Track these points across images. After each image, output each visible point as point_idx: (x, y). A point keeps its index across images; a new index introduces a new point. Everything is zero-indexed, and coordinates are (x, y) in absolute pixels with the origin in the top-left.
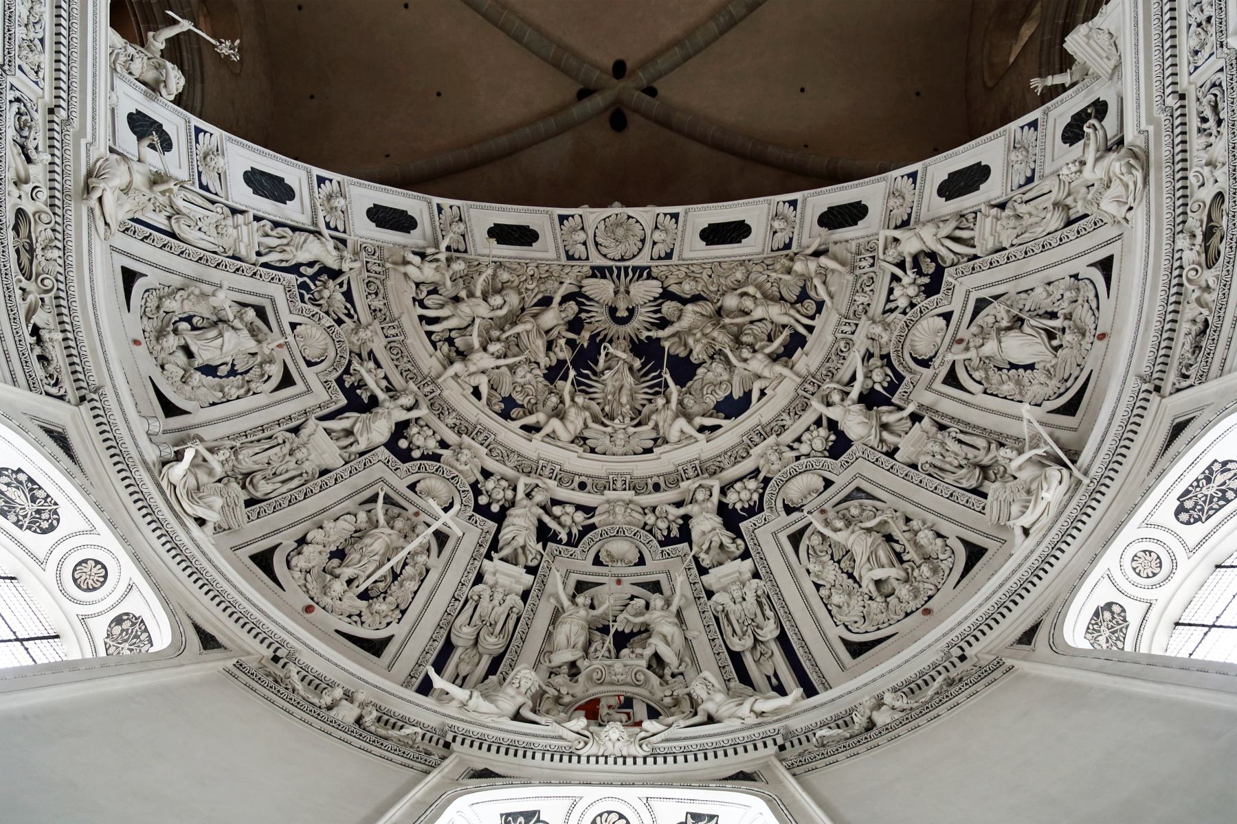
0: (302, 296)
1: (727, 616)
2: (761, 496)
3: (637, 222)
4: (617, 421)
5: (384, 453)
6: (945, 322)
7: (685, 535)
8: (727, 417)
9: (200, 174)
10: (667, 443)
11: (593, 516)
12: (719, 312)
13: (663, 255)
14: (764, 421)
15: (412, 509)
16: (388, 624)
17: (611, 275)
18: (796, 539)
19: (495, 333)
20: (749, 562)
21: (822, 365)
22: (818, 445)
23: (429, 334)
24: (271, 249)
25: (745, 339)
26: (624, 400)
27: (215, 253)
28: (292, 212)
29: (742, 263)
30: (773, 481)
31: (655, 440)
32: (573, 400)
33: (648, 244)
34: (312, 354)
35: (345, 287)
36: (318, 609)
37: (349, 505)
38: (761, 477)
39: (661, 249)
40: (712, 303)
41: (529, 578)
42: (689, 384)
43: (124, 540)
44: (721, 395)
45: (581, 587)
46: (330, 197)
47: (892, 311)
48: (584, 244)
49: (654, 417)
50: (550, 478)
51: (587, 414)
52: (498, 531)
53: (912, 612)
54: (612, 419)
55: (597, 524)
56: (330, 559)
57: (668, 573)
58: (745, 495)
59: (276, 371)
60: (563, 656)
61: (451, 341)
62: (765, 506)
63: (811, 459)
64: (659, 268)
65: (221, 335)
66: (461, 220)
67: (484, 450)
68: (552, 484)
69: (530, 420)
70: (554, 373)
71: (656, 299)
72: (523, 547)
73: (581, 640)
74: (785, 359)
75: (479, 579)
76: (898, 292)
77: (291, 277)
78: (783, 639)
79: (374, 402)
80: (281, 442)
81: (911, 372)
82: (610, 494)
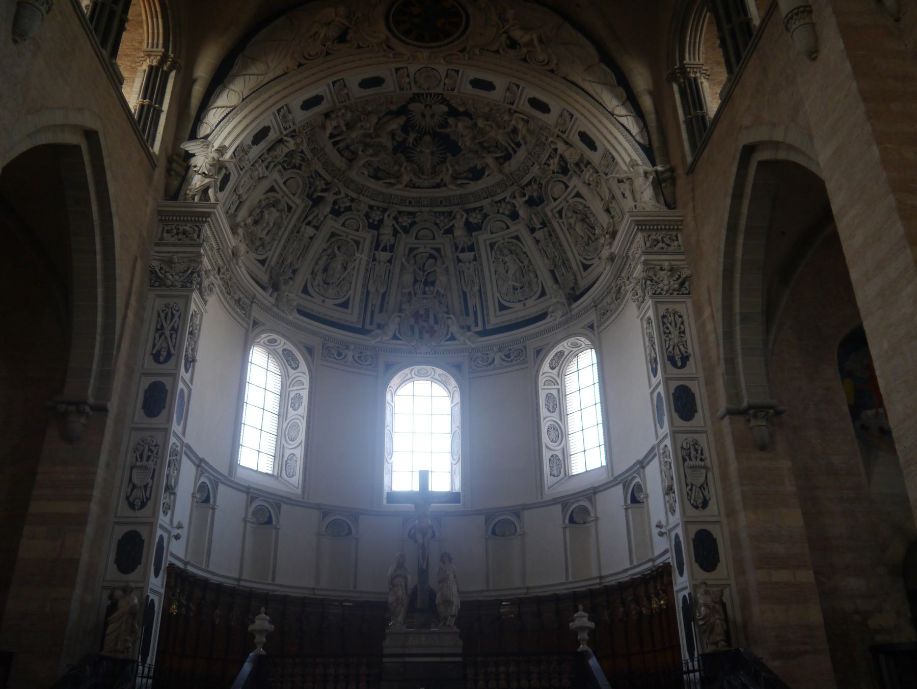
0: (283, 167)
1: (463, 272)
3: (437, 71)
4: (425, 177)
5: (330, 216)
6: (564, 189)
7: (450, 231)
9: (240, 167)
10: (445, 186)
11: (414, 218)
12: (476, 124)
13: (450, 89)
16: (347, 291)
17: (423, 96)
18: (492, 245)
19: (368, 140)
20: (474, 253)
22: (507, 212)
24: (270, 163)
25: (485, 144)
28: (272, 136)
30: (487, 219)
31: (442, 180)
32: (405, 168)
33: (442, 83)
36: (327, 300)
38: (483, 212)
40: (471, 119)
41: (392, 254)
42: (459, 156)
43: (278, 333)
45: (412, 250)
46: (284, 116)
48: (409, 83)
50: (396, 204)
52: (379, 235)
53: (521, 301)
54: (423, 174)
56: (323, 273)
58: (476, 221)
60: (406, 291)
63: (504, 216)
66: (345, 86)
69: (388, 181)
70: (395, 150)
71: (444, 112)
72: (389, 240)
73: (412, 280)
74: (501, 161)
75: (374, 260)
78: (480, 291)
80: (295, 238)
82: (423, 209)
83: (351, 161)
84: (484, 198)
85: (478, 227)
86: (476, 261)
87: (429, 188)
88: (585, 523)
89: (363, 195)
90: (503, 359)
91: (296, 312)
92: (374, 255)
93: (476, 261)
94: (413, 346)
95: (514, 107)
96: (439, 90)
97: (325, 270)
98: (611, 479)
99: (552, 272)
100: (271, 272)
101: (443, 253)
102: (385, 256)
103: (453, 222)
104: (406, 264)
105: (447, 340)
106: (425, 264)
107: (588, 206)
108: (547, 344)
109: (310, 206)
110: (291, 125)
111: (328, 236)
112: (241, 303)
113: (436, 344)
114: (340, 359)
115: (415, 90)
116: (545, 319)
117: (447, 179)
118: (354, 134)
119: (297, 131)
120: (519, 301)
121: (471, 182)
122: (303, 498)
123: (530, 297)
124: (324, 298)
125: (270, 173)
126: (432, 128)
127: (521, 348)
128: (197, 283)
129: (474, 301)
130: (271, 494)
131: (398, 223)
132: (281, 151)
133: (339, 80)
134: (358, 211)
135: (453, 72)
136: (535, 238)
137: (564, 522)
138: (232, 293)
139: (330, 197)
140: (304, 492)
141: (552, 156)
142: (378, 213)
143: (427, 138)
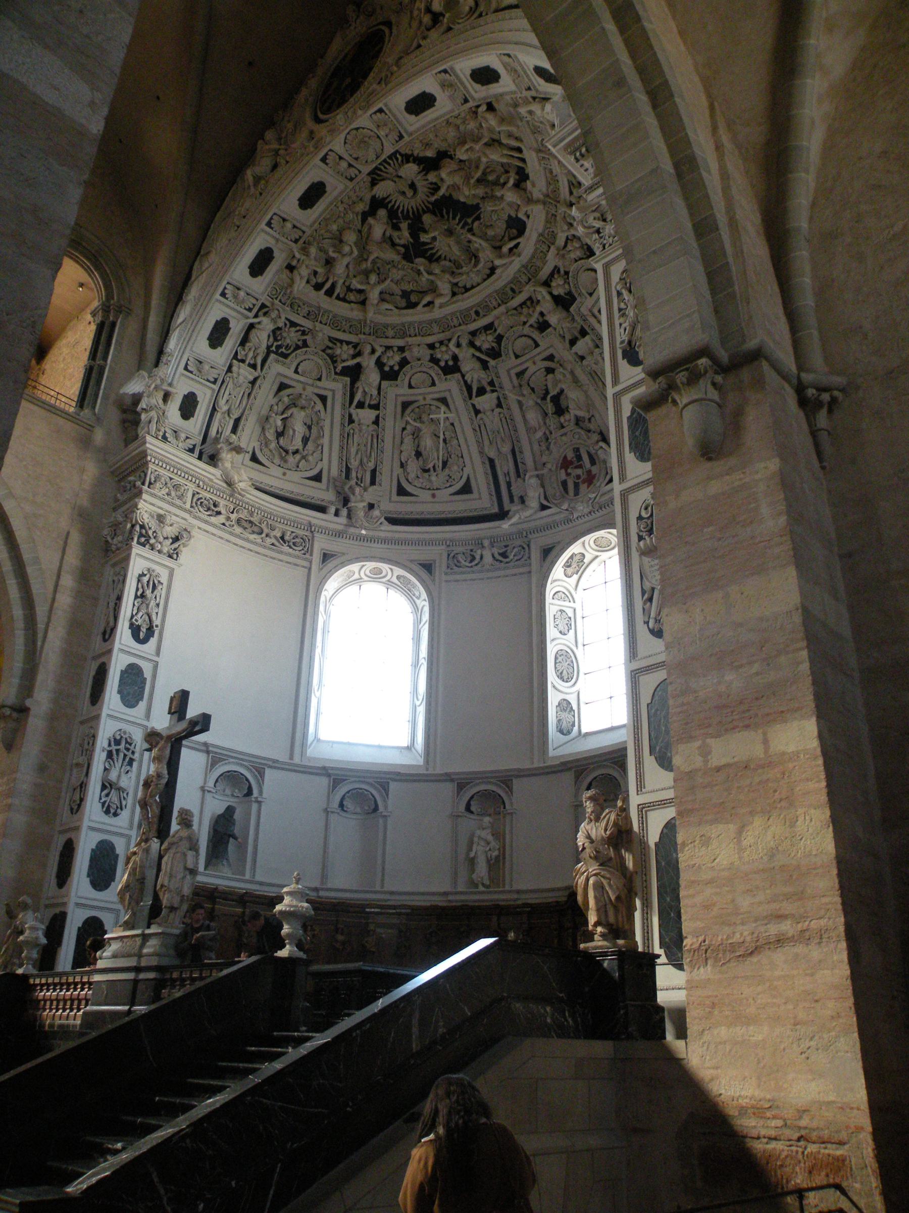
4: (464, 269)
5: (385, 384)
9: (208, 380)
11: (496, 330)
13: (397, 139)
14: (540, 231)
15: (420, 398)
17: (381, 170)
23: (338, 298)
25: (491, 178)
26: (458, 253)
27: (249, 395)
28: (237, 327)
34: (315, 374)
35: (287, 323)
37: (400, 424)
38: (562, 272)
46: (235, 297)
48: (350, 165)
50: (460, 325)
51: (447, 276)
52: (463, 376)
54: (459, 267)
55: (502, 333)
56: (418, 459)
59: (319, 406)
60: (539, 434)
61: (349, 289)
64: (402, 146)
65: (294, 431)
66: (284, 220)
67: (419, 338)
68: (462, 327)
69: (424, 302)
75: (477, 412)
77: (272, 356)
79: (359, 366)
82: (496, 312)
83: (363, 303)
87: (485, 280)
89: (410, 336)
91: (386, 523)
92: (474, 406)
94: (567, 510)
95: (471, 104)
96: (389, 150)
97: (418, 454)
100: (336, 486)
102: (486, 402)
103: (538, 309)
104: (520, 398)
106: (546, 385)
109: (349, 383)
110: (254, 301)
111: (399, 409)
112: (287, 538)
113: (594, 495)
114: (476, 565)
115: (366, 169)
118: (340, 269)
119: (268, 304)
122: (427, 770)
124: (431, 492)
125: (262, 369)
126: (428, 202)
128: (141, 535)
130: (368, 771)
131: (479, 349)
132: (261, 338)
133: (271, 218)
134: (419, 360)
135: (378, 114)
138: (266, 531)
139: (368, 362)
140: (427, 761)
143: (427, 219)
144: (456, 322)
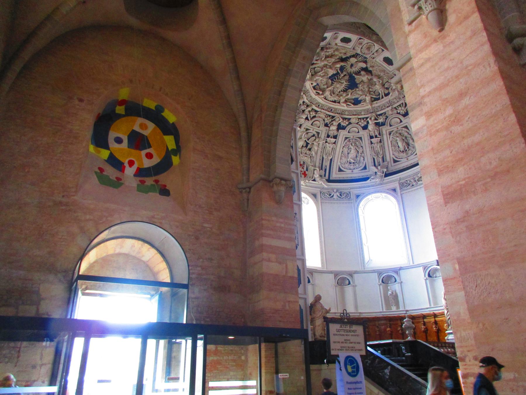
2: (348, 125)
4: (334, 95)
8: (354, 104)
10: (339, 103)
11: (316, 114)
13: (372, 58)
18: (346, 138)
20: (335, 140)
21: (377, 106)
22: (363, 125)
29: (384, 71)
38: (349, 121)
39: (373, 56)
44: (357, 96)
47: (396, 109)
49: (341, 97)
50: (314, 104)
54: (334, 93)
57: (322, 131)
58: (344, 125)
62: (346, 129)
63: (359, 126)
69: (318, 92)
76: (400, 108)
78: (331, 160)
81: (387, 125)
82: (322, 111)
84: (354, 115)
85: (344, 128)
86: (335, 144)
87: (330, 101)
88: (387, 284)
89: (305, 95)
90: (338, 196)
93: (335, 144)
96: (368, 56)
98: (411, 264)
99: (374, 159)
101: (320, 136)
105: (312, 181)
106: (309, 138)
107: (410, 134)
108: (364, 194)
115: (359, 52)
116: (366, 181)
117: (343, 100)
120: (350, 169)
121: (352, 105)
123: (357, 168)
126: (350, 73)
127: (347, 192)
129: (326, 164)
136: (371, 142)
137: (379, 282)
141: (401, 105)
142: (306, 106)
143: (347, 78)
144: (314, 103)
